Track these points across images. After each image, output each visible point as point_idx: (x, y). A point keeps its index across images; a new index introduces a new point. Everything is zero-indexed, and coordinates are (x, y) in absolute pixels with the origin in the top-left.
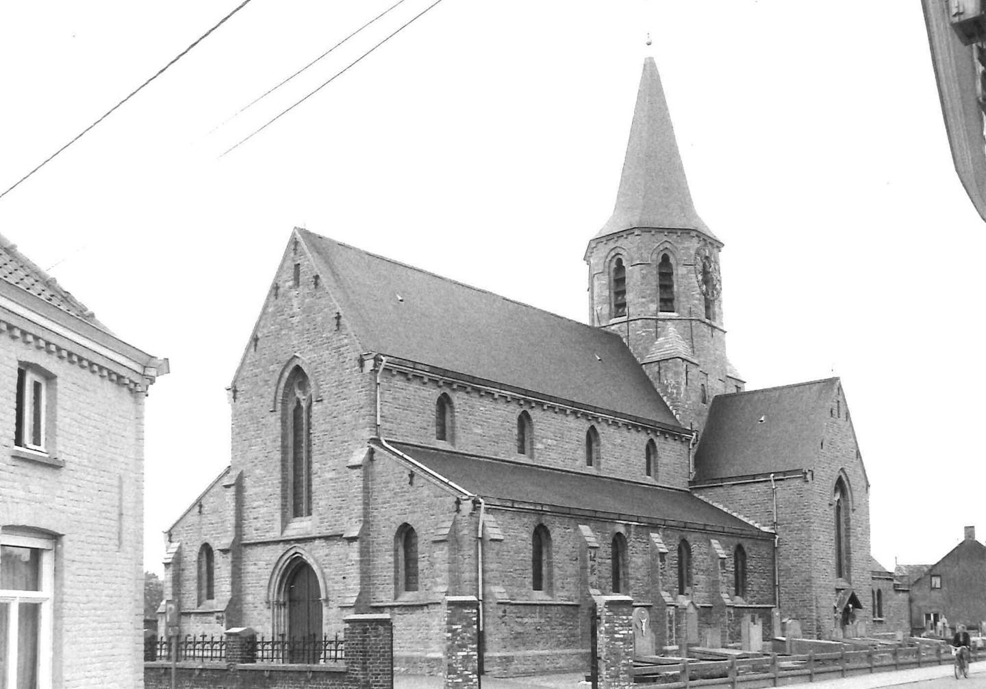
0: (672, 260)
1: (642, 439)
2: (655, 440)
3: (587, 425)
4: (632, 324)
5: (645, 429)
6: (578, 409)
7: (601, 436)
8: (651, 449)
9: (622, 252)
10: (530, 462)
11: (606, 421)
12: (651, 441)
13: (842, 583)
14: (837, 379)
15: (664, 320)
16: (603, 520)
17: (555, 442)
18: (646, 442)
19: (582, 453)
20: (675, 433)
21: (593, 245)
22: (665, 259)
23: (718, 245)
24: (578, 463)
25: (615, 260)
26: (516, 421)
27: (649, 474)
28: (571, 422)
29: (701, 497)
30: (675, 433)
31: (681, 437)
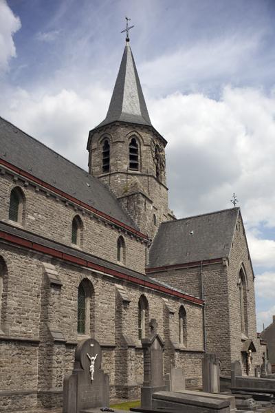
0: (137, 142)
1: (116, 235)
2: (124, 237)
3: (74, 214)
4: (112, 177)
5: (117, 228)
6: (66, 199)
7: (84, 224)
8: (121, 242)
9: (109, 137)
10: (21, 227)
11: (89, 214)
12: (121, 237)
13: (244, 337)
14: (238, 208)
15: (132, 174)
16: (70, 263)
17: (45, 218)
18: (117, 237)
19: (68, 231)
20: (137, 235)
21: (92, 134)
22: (133, 143)
23: (164, 142)
24: (64, 238)
25: (104, 141)
26: (9, 192)
27: (119, 260)
28: (61, 208)
29: (154, 279)
30: (137, 235)
31: (141, 240)
